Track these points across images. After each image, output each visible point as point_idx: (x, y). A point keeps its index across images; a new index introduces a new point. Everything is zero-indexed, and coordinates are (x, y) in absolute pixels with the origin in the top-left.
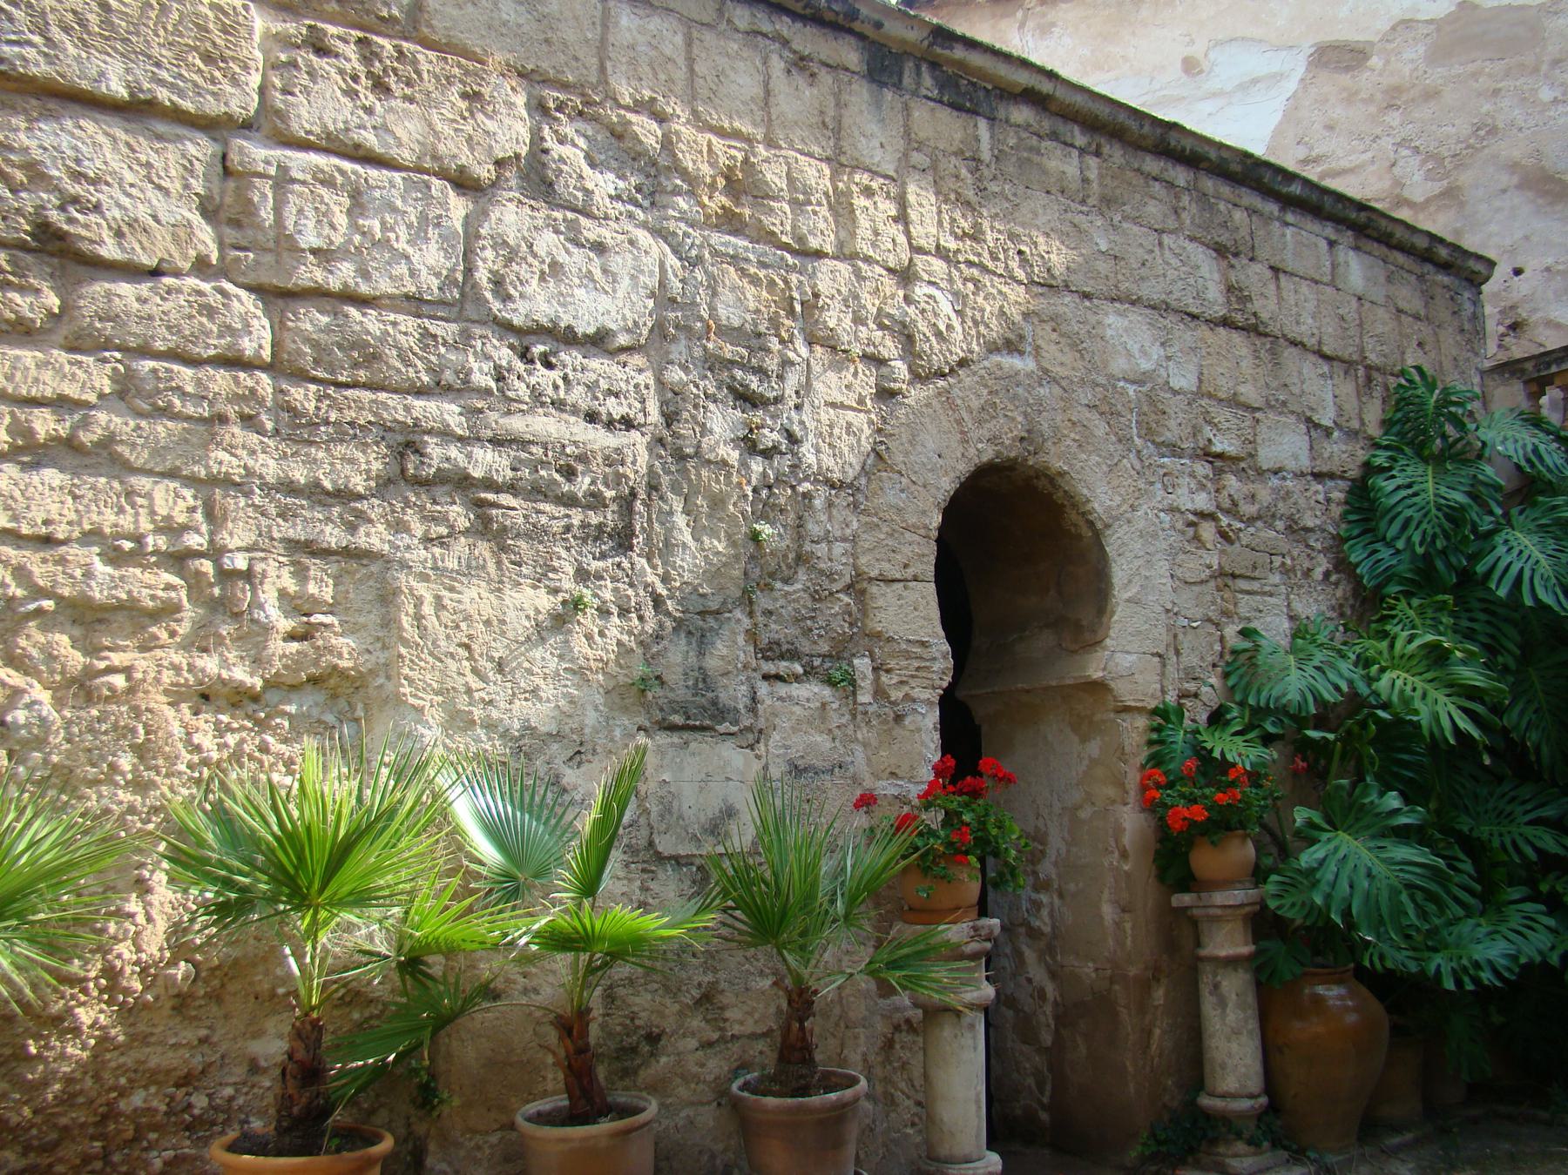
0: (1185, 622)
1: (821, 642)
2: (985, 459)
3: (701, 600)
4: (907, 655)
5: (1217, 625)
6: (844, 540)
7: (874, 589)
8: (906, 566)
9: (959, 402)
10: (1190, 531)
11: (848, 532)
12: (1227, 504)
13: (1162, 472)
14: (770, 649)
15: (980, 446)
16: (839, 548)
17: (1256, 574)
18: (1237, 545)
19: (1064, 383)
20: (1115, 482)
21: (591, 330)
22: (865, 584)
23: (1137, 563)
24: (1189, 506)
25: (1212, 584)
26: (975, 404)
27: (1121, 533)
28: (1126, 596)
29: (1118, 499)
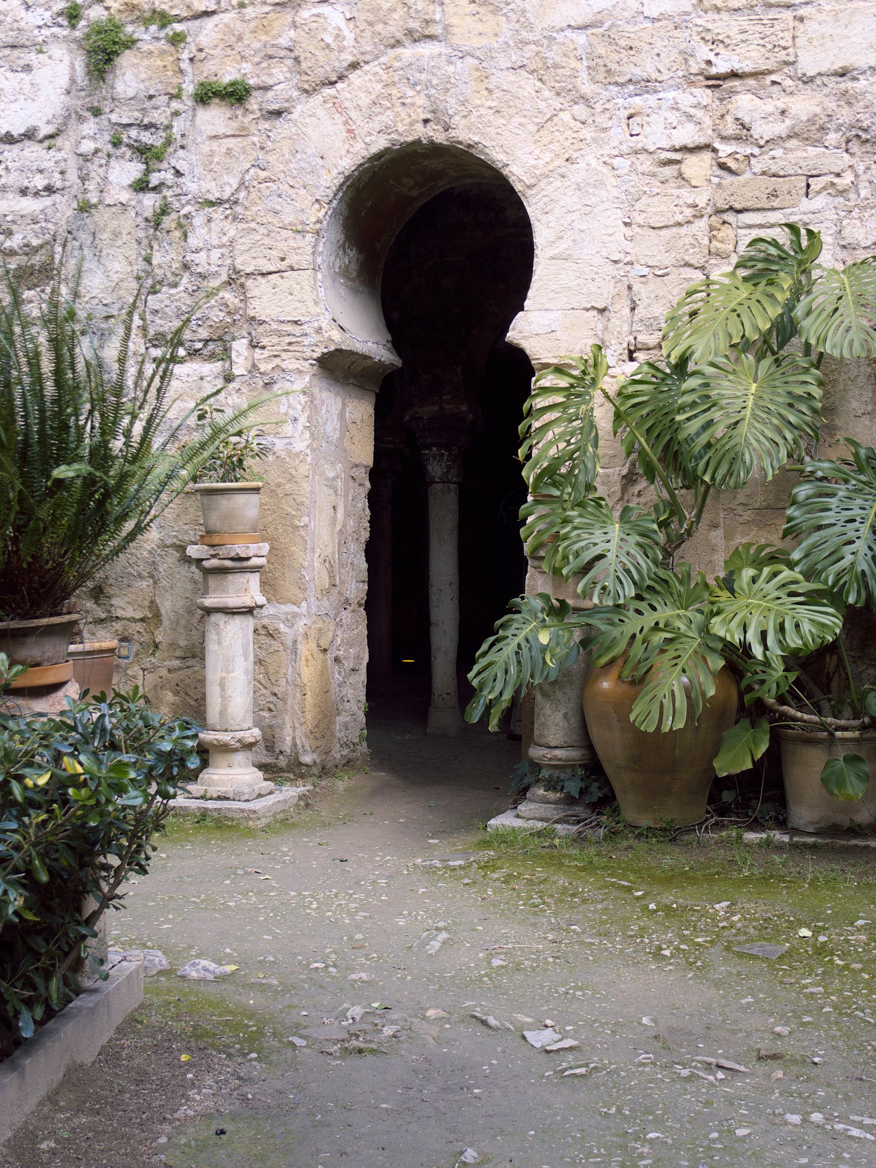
0: (645, 271)
1: (200, 330)
2: (374, 150)
3: (106, 308)
5: (703, 268)
7: (249, 283)
8: (283, 259)
9: (347, 104)
10: (669, 171)
11: (225, 239)
12: (731, 128)
13: (627, 113)
14: (157, 339)
16: (215, 254)
17: (775, 204)
18: (748, 175)
19: (478, 53)
20: (546, 140)
21: (22, 131)
22: (243, 280)
23: (569, 218)
24: (666, 144)
25: (702, 224)
26: (365, 101)
27: (550, 188)
28: (551, 253)
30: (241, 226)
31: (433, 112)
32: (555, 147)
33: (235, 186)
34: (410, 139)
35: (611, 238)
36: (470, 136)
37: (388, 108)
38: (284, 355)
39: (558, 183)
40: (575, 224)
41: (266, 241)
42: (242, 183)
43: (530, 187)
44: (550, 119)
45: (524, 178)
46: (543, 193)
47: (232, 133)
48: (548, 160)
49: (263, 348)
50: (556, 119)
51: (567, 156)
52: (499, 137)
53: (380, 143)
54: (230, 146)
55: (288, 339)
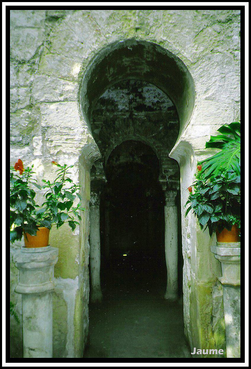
2: (110, 41)
4: (61, 134)
6: (25, 86)
7: (42, 107)
11: (28, 82)
15: (107, 35)
28: (204, 97)
29: (202, 48)
30: (37, 76)
31: (140, 24)
32: (205, 44)
33: (33, 53)
34: (130, 37)
35: (235, 90)
36: (162, 37)
37: (118, 20)
38: (63, 145)
39: (207, 62)
40: (217, 82)
41: (53, 85)
42: (36, 53)
43: (194, 63)
44: (202, 30)
45: (190, 59)
46: (200, 67)
47: (31, 25)
48: (202, 50)
49: (52, 141)
50: (205, 31)
51: (211, 49)
52: (177, 38)
53: (113, 38)
54: (30, 32)
55: (65, 137)
